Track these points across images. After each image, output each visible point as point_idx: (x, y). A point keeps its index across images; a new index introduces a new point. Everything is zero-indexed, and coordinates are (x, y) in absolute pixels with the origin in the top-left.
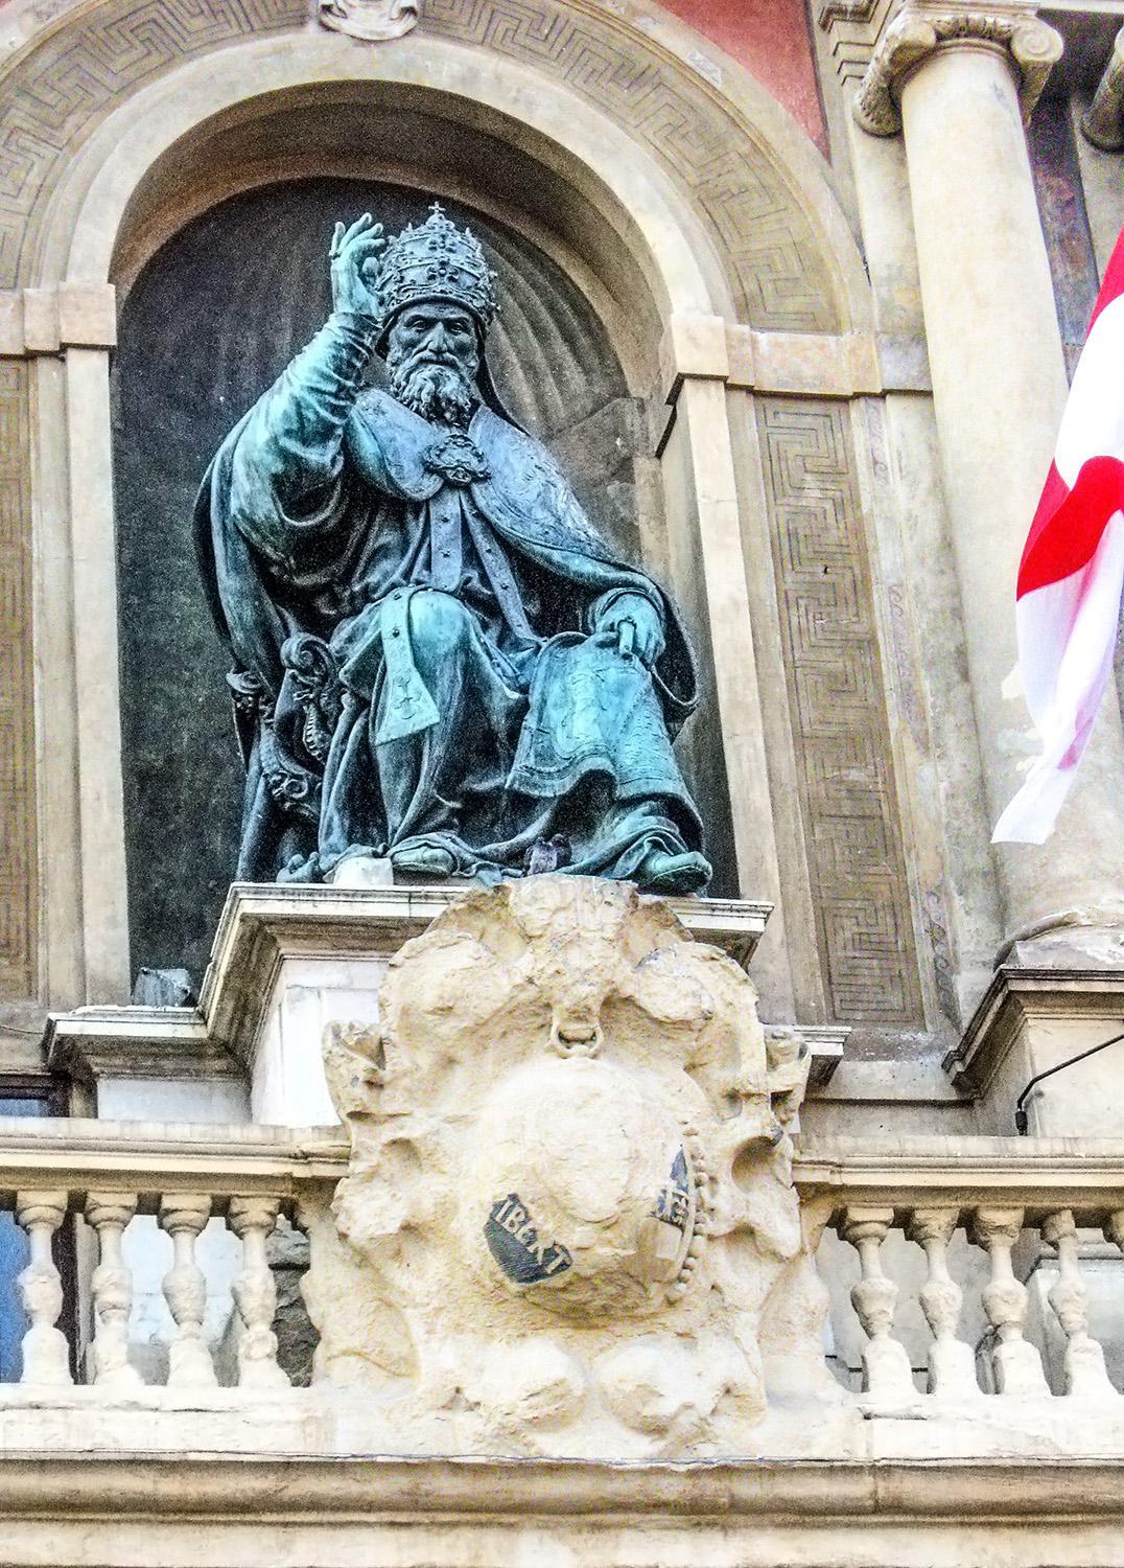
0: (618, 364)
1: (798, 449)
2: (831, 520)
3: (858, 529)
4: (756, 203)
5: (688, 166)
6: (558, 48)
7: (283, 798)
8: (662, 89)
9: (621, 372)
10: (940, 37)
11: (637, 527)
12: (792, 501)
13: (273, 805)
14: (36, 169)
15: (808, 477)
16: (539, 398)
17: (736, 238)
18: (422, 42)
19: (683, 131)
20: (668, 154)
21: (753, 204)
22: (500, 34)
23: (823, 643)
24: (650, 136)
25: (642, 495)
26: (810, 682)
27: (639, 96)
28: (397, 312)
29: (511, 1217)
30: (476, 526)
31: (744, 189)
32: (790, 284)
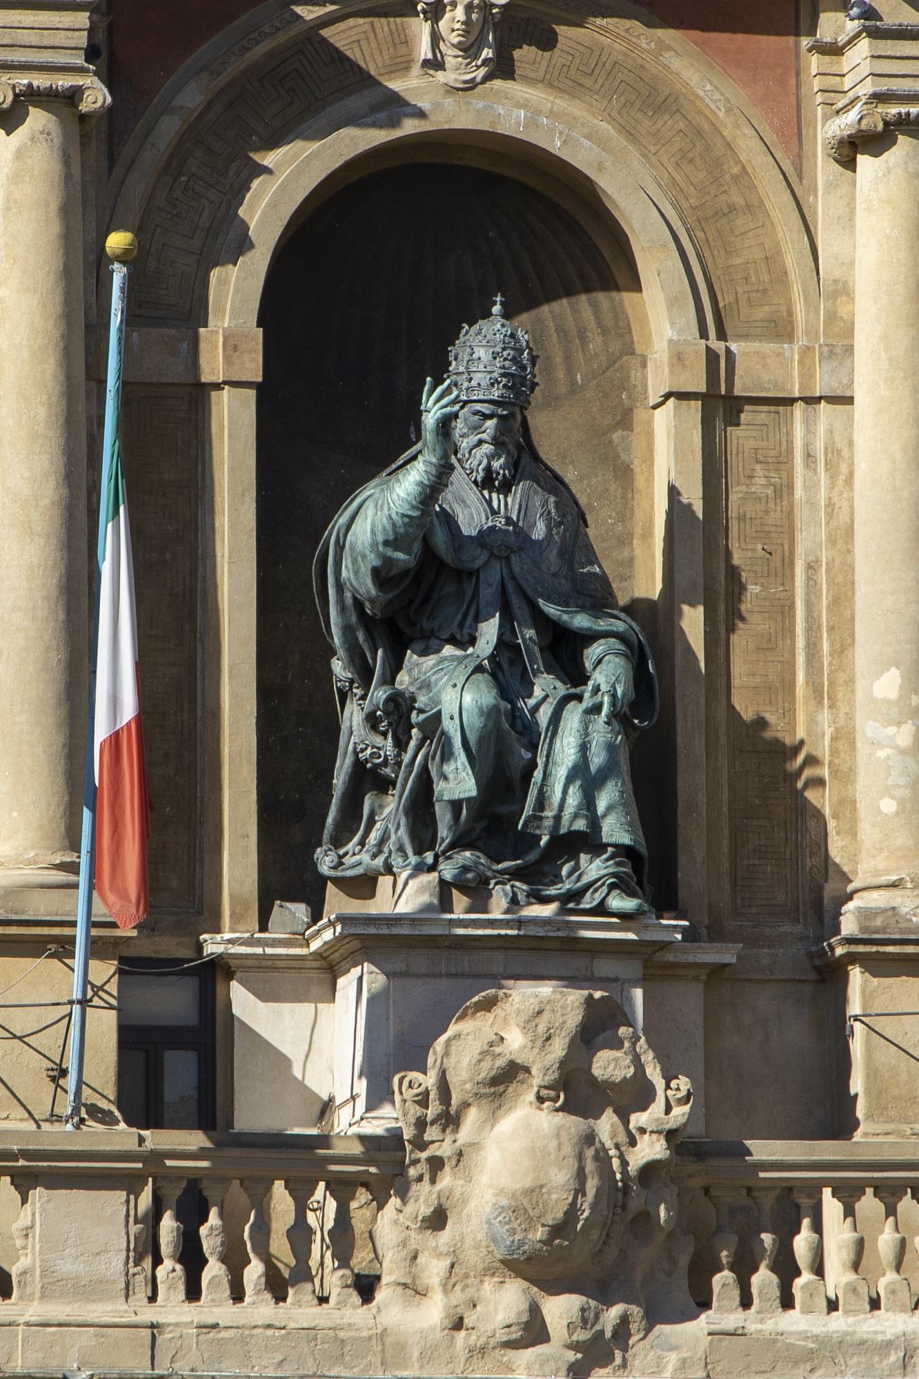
0: (629, 325)
1: (752, 443)
2: (771, 505)
3: (790, 514)
4: (742, 222)
5: (692, 188)
6: (600, 81)
7: (367, 761)
8: (677, 116)
9: (630, 332)
10: (886, 124)
11: (632, 470)
12: (744, 488)
13: (358, 765)
14: (206, 213)
15: (758, 467)
16: (568, 358)
17: (723, 253)
18: (497, 84)
19: (690, 156)
20: (678, 178)
21: (739, 222)
22: (556, 72)
23: (756, 609)
24: (664, 160)
25: (637, 441)
26: (744, 642)
27: (659, 125)
28: (466, 403)
29: (500, 1218)
30: (510, 586)
31: (732, 209)
32: (760, 295)
